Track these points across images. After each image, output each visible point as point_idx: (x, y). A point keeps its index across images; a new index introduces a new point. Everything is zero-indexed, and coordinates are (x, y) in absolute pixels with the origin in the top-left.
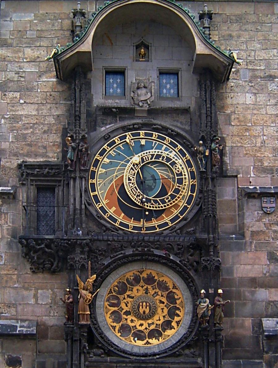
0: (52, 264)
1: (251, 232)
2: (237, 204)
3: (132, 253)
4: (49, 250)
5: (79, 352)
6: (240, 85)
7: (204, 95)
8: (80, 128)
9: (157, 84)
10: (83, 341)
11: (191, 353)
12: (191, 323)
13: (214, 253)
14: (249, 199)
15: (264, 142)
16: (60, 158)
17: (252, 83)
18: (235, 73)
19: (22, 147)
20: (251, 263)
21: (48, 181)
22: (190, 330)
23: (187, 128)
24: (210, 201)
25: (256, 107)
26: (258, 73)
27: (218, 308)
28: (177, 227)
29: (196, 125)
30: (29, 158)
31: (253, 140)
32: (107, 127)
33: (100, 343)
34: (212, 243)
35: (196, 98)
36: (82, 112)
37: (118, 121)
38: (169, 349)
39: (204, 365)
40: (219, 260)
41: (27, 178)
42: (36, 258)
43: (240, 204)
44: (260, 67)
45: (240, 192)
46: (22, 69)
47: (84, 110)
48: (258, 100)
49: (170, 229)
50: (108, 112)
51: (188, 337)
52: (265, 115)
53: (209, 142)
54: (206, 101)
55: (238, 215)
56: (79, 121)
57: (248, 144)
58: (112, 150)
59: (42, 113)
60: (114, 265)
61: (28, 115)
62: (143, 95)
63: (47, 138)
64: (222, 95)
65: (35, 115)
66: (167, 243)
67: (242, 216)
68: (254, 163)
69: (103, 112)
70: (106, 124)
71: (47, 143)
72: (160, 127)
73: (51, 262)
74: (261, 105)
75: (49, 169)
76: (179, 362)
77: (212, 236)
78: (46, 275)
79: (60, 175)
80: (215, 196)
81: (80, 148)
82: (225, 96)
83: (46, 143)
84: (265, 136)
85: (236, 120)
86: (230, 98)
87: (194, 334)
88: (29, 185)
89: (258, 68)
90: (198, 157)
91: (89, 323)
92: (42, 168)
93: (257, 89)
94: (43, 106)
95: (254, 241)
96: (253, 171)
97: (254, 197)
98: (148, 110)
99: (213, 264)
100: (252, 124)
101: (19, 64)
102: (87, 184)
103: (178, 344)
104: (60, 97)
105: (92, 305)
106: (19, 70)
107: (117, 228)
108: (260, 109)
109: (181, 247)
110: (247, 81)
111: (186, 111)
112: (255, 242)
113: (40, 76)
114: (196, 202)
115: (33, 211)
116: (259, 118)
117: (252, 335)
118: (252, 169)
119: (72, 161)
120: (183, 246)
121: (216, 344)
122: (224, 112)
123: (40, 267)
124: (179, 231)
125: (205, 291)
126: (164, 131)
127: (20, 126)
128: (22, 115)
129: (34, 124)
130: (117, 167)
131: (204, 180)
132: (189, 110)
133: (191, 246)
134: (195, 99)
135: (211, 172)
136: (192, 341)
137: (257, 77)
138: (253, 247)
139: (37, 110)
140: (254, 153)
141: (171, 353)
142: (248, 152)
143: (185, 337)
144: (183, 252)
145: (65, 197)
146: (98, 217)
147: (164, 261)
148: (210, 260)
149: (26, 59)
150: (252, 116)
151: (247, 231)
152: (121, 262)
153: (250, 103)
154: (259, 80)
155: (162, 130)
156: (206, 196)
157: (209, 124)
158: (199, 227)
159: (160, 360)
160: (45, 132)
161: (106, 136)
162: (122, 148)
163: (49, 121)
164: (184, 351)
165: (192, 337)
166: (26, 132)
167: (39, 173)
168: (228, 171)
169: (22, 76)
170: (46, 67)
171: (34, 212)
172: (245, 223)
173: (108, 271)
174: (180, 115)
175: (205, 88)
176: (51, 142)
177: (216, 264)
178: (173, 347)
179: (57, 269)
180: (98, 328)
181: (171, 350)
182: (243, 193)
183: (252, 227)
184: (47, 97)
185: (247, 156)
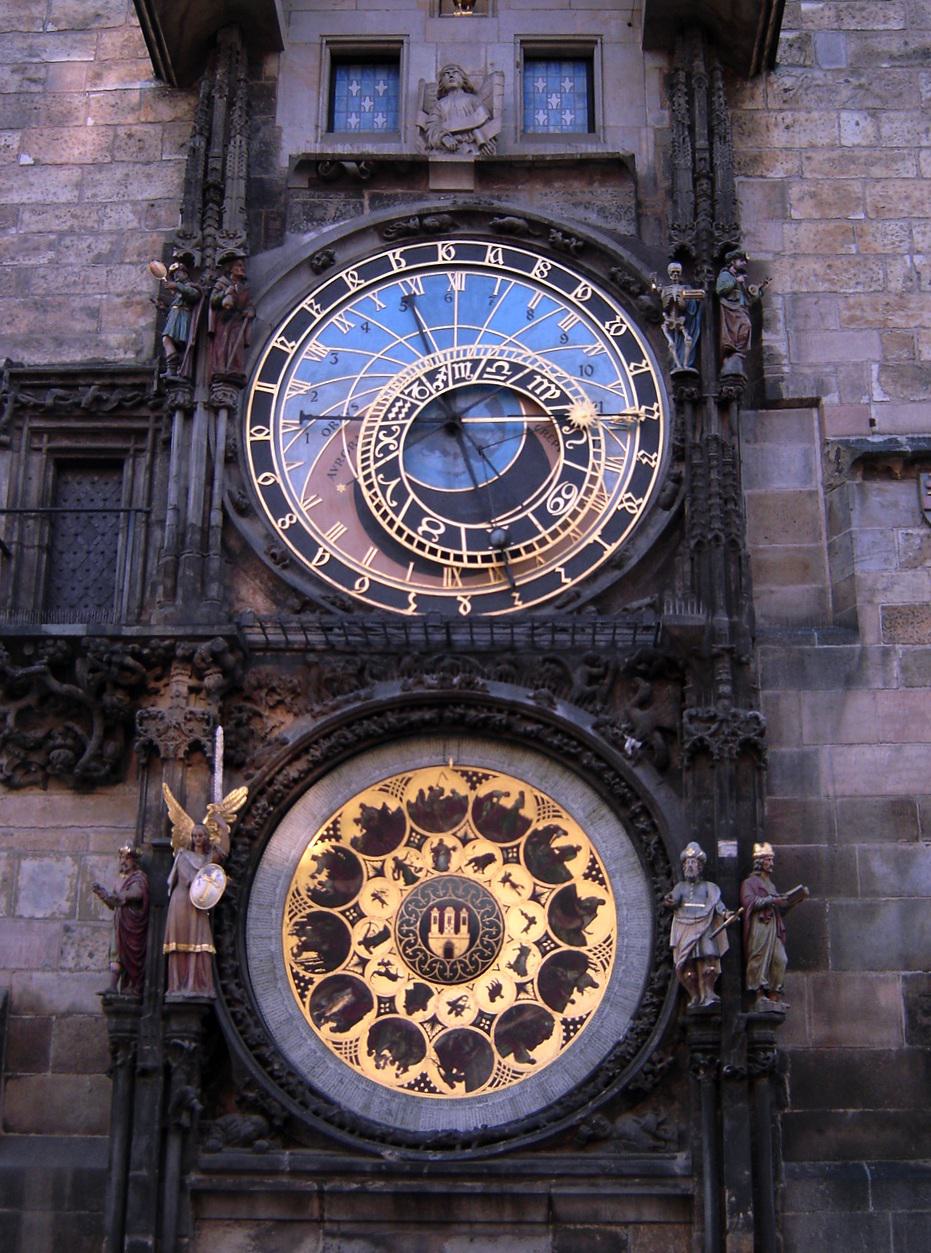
0: (79, 750)
1: (883, 608)
2: (822, 508)
3: (398, 693)
4: (66, 687)
5: (157, 1127)
6: (818, 85)
7: (685, 106)
8: (220, 226)
9: (515, 91)
10: (178, 1076)
11: (645, 1129)
12: (643, 996)
13: (735, 691)
14: (868, 484)
15: (915, 276)
16: (146, 350)
17: (861, 75)
18: (796, 45)
19: (11, 315)
20: (891, 736)
21: (95, 433)
22: (642, 1024)
23: (625, 228)
24: (715, 483)
25: (877, 154)
26: (883, 45)
27: (761, 920)
28: (588, 593)
29: (659, 220)
30: (32, 354)
31: (876, 269)
32: (325, 230)
33: (251, 1084)
34: (727, 646)
35: (656, 131)
36: (229, 174)
37: (367, 211)
38: (550, 1113)
39: (701, 1184)
40: (757, 718)
41: (20, 423)
42: (10, 720)
43: (837, 504)
44: (885, 23)
45: (832, 456)
46: (38, 56)
47: (236, 166)
48: (886, 130)
49: (558, 603)
50: (328, 175)
51: (633, 1056)
52: (916, 182)
53: (706, 267)
54: (691, 129)
55: (830, 547)
56: (220, 204)
57: (857, 283)
58: (341, 312)
59: (95, 196)
60: (326, 744)
61: (43, 205)
62: (457, 112)
63: (104, 278)
64: (752, 119)
65: (69, 204)
66: (547, 656)
67: (843, 552)
68: (883, 351)
69: (310, 180)
70: (322, 221)
71: (105, 296)
72: (521, 222)
73: (76, 737)
74: (898, 148)
75: (103, 387)
76: (592, 1171)
77: (726, 619)
78: (56, 797)
79: (144, 412)
80: (734, 466)
81: (214, 297)
82: (763, 122)
83: (99, 297)
84: (919, 252)
85: (809, 203)
86: (783, 126)
87: (656, 1040)
88: (23, 448)
89: (881, 27)
90: (664, 328)
91: (208, 992)
92: (75, 387)
93: (878, 97)
94: (100, 172)
95: (897, 646)
96: (878, 380)
97: (889, 474)
98: (477, 163)
99: (734, 734)
100: (866, 214)
101: (29, 41)
102: (238, 437)
103: (590, 1088)
104: (162, 140)
105: (228, 917)
106: (28, 59)
107: (345, 599)
108: (894, 160)
109: (602, 670)
110: (840, 71)
111: (617, 167)
112: (900, 652)
113: (98, 76)
114: (658, 498)
115: (33, 547)
116: (891, 193)
117: (906, 1046)
118: (875, 374)
119: (179, 346)
120: (607, 668)
121: (751, 1088)
122: (762, 177)
123: (31, 763)
124: (592, 608)
125: (703, 848)
126: (536, 237)
127: (13, 243)
128: (23, 204)
129: (62, 235)
130: (358, 373)
131: (688, 409)
132: (629, 165)
133: (641, 667)
134: (652, 136)
135: (717, 380)
136: (646, 1074)
137: (872, 55)
138: (896, 672)
139: (79, 186)
140: (880, 317)
141: (561, 1128)
142: (858, 313)
143: (620, 1057)
144: (611, 691)
145: (156, 491)
146: (273, 556)
147: (529, 728)
148: (721, 715)
149: (55, 22)
150: (865, 185)
151: (869, 608)
152: (353, 731)
153: (856, 142)
154: (884, 65)
155: (527, 234)
156: (699, 466)
157: (704, 205)
158: (674, 591)
159: (508, 1162)
160: (98, 260)
161: (318, 259)
162: (378, 302)
163: (118, 224)
164: (612, 1121)
165: (648, 1054)
166: (32, 262)
167: (62, 402)
168: (783, 385)
169: (35, 76)
170: (124, 47)
171: (36, 549)
172: (858, 574)
173: (301, 772)
174: (596, 184)
175: (688, 85)
176: (119, 295)
177: (742, 735)
178: (568, 1104)
179: (96, 770)
180: (249, 1020)
181: (557, 1118)
182: (846, 460)
183: (885, 589)
184: (118, 143)
185: (852, 327)
